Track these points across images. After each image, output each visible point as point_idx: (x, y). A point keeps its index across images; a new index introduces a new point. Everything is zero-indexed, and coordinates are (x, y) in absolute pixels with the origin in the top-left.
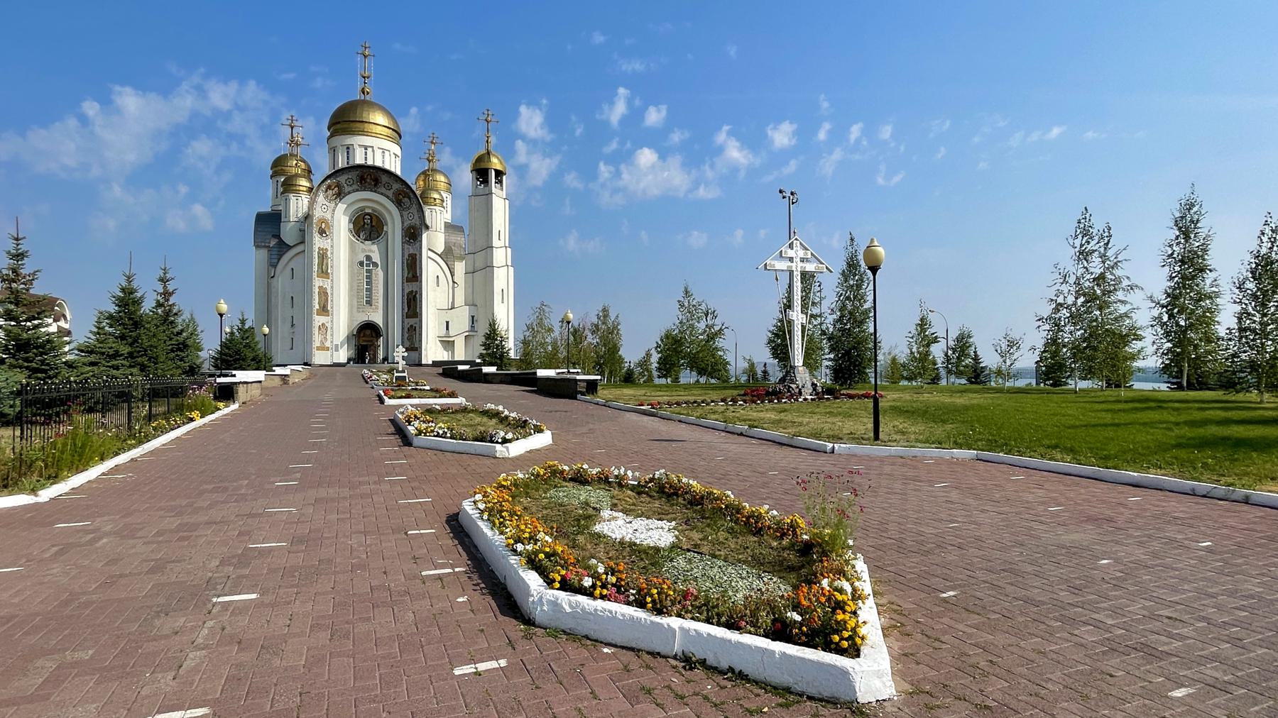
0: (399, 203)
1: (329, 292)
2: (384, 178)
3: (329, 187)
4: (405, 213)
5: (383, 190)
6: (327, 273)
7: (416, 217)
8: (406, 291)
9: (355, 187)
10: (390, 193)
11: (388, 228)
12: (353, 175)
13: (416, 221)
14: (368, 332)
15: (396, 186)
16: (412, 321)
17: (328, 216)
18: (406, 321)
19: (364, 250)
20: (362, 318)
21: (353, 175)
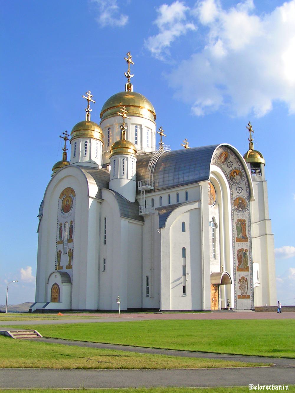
0: (231, 179)
4: (234, 187)
10: (228, 170)
15: (236, 165)
18: (238, 273)
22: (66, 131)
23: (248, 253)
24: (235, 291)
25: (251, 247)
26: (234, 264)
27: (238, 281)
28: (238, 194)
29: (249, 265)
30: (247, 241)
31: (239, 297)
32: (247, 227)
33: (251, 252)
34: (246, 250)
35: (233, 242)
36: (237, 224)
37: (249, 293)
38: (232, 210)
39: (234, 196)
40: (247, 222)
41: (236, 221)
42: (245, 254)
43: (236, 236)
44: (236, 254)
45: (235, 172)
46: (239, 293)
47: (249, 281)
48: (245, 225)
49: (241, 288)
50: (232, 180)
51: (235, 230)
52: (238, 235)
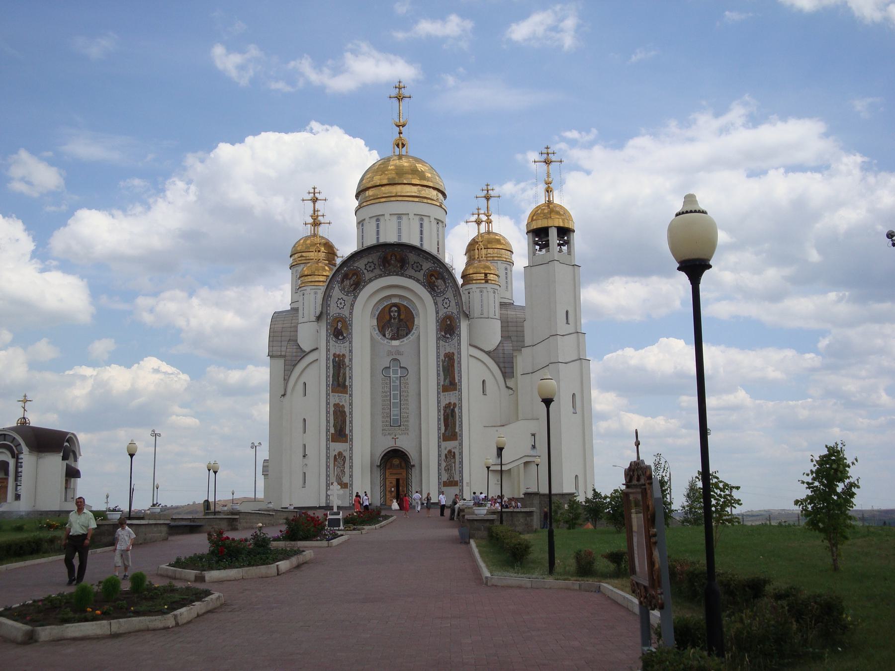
0: (431, 287)
1: (347, 410)
2: (412, 257)
3: (346, 277)
4: (440, 300)
5: (411, 272)
6: (345, 386)
7: (453, 303)
8: (443, 404)
9: (377, 272)
10: (420, 275)
11: (419, 321)
12: (374, 257)
13: (453, 309)
14: (396, 462)
15: (427, 265)
16: (450, 445)
17: (346, 312)
19: (390, 353)
20: (387, 444)
21: (374, 257)
22: (547, 148)
23: (456, 410)
24: (439, 474)
25: (460, 399)
26: (439, 429)
27: (443, 457)
28: (445, 310)
29: (457, 430)
30: (455, 389)
31: (446, 484)
32: (456, 365)
33: (461, 408)
34: (455, 404)
35: (438, 393)
36: (443, 362)
37: (457, 478)
38: (438, 339)
39: (440, 314)
40: (455, 357)
41: (442, 357)
42: (453, 411)
43: (442, 383)
44: (442, 412)
45: (432, 275)
46: (445, 477)
47: (457, 456)
48: (454, 362)
49: (448, 469)
50: (434, 290)
51: (442, 373)
52: (445, 380)
